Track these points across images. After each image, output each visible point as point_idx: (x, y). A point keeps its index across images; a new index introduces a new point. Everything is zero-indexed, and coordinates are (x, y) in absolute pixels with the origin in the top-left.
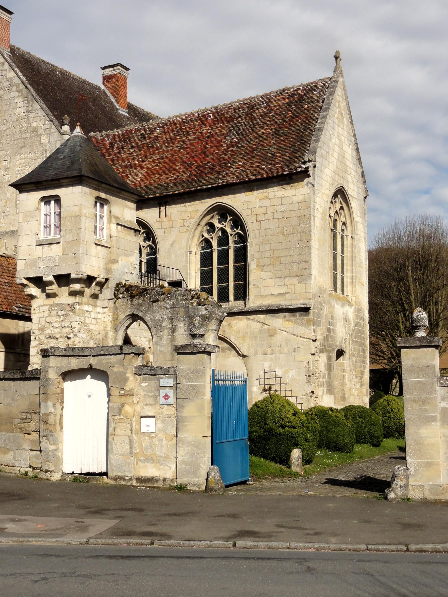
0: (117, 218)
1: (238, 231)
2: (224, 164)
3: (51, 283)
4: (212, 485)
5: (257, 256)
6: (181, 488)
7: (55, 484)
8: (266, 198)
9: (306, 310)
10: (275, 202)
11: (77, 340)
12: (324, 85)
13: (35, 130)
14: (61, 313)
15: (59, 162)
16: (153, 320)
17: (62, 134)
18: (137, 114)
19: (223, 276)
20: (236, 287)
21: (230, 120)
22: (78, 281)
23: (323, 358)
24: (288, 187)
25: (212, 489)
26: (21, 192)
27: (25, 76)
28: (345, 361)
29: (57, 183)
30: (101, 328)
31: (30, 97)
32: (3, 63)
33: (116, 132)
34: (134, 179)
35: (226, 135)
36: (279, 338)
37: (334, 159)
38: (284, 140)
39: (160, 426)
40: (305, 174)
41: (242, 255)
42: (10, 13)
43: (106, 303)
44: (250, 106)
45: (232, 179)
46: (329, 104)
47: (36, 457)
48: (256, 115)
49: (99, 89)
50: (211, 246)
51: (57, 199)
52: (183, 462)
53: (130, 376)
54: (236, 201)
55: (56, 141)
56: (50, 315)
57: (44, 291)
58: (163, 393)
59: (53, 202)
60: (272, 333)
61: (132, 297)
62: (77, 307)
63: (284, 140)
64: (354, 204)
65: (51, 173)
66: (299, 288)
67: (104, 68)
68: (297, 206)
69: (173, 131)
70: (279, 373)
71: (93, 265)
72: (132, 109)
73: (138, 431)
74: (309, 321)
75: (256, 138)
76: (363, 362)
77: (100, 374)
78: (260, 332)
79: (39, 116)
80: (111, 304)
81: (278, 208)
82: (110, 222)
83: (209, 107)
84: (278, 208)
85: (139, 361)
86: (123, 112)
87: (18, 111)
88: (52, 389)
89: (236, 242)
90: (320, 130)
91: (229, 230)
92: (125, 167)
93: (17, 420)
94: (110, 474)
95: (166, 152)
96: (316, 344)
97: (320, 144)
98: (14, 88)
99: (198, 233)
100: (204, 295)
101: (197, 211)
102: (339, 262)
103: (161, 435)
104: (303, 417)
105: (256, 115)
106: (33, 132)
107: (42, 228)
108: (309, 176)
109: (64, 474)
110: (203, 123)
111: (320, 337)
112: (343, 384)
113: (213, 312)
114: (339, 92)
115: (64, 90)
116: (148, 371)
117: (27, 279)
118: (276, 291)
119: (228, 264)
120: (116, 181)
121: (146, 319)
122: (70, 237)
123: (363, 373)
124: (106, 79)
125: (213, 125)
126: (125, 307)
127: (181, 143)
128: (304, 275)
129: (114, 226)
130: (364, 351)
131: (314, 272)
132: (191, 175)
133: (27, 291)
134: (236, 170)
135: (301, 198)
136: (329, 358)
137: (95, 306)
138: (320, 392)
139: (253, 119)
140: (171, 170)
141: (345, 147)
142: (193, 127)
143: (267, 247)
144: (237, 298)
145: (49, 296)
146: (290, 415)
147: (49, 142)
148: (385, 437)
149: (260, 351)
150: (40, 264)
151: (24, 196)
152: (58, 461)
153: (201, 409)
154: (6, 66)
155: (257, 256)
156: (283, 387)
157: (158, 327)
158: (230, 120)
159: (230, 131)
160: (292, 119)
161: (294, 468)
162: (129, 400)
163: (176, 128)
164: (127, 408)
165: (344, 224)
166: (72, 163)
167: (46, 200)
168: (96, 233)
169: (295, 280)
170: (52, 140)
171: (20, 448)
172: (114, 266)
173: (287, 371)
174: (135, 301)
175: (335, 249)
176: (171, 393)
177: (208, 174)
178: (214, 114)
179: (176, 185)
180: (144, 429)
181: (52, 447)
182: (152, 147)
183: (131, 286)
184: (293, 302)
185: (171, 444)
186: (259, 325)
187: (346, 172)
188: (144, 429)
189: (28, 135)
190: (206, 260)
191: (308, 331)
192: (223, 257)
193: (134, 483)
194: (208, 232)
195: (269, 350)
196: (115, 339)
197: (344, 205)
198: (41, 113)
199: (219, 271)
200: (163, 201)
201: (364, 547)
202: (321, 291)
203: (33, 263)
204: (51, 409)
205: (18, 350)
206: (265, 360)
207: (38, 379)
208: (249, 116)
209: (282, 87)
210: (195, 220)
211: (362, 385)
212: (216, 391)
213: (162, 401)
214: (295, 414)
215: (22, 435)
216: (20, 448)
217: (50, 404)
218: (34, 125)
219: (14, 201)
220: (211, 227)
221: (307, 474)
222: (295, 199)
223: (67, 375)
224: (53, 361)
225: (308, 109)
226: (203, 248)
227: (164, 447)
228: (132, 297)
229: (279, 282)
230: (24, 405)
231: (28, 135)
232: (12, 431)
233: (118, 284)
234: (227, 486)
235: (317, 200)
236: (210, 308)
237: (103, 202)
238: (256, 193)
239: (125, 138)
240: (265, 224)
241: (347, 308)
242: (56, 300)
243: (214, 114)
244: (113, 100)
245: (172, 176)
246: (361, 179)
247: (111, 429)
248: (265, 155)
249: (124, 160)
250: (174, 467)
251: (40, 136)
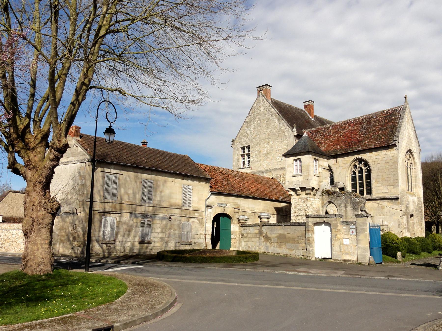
0: (321, 166)
1: (367, 168)
2: (360, 142)
3: (298, 190)
4: (370, 263)
5: (375, 177)
6: (359, 264)
7: (313, 261)
8: (378, 155)
9: (397, 199)
10: (382, 156)
11: (309, 211)
12: (400, 109)
13: (282, 131)
14: (302, 201)
15: (300, 146)
16: (338, 204)
17: (293, 132)
18: (321, 121)
19: (361, 185)
20: (367, 190)
21: (361, 124)
22: (309, 189)
23: (405, 218)
24: (388, 150)
25: (371, 264)
26: (286, 157)
27: (277, 110)
28: (414, 219)
29: (300, 154)
30: (317, 206)
31: (280, 118)
33: (313, 129)
34: (323, 148)
35: (360, 130)
36: (386, 210)
37: (406, 138)
38: (385, 132)
39: (351, 242)
40: (395, 145)
41: (369, 177)
42: (271, 86)
43: (319, 197)
44: (369, 118)
45: (364, 148)
46: (403, 117)
47: (305, 252)
48: (372, 121)
49: (303, 111)
50: (356, 174)
51: (300, 160)
52: (360, 255)
53: (339, 224)
54: (365, 156)
56: (298, 202)
57: (296, 193)
58: (351, 230)
59: (298, 161)
60: (383, 208)
61: (329, 195)
62: (309, 199)
63: (385, 132)
64: (415, 155)
65: (297, 151)
66: (394, 190)
67: (304, 102)
68: (391, 158)
69: (337, 128)
70: (387, 223)
71: (314, 183)
72: (316, 117)
73: (343, 244)
74: (399, 203)
75: (373, 131)
76: (422, 219)
77: (328, 224)
78: (378, 207)
79: (284, 126)
80: (321, 197)
81: (384, 159)
82: (319, 167)
83: (351, 118)
84: (384, 159)
85: (341, 220)
86: (313, 119)
87: (275, 123)
88: (310, 229)
89: (366, 172)
90: (400, 127)
91: (363, 167)
92: (318, 143)
93: (296, 239)
94: (333, 258)
95: (335, 137)
96: (402, 212)
97: (400, 133)
99: (350, 169)
100: (354, 193)
101: (349, 160)
102: (410, 179)
103: (351, 245)
104: (400, 240)
105: (372, 121)
107: (294, 170)
108: (396, 146)
109: (316, 258)
110: (349, 125)
111: (403, 209)
112: (413, 228)
113: (362, 201)
114: (407, 111)
115: (291, 113)
116: (346, 223)
117: (290, 189)
118: (384, 191)
119: (363, 181)
120: (320, 152)
121: (335, 203)
122: (305, 174)
123: (422, 224)
124: (305, 106)
125: (354, 126)
126: (326, 198)
127: (341, 133)
128: (396, 185)
129: (320, 169)
130: (422, 215)
131: (400, 183)
132: (346, 146)
133: (289, 193)
134: (365, 144)
135: (393, 155)
136: (407, 218)
137: (315, 198)
138: (404, 231)
139: (370, 123)
140: (338, 144)
141: (410, 133)
142: (345, 127)
143: (380, 174)
144: (367, 194)
145: (298, 195)
146: (396, 239)
148: (433, 250)
149: (378, 215)
150: (294, 183)
151: (287, 159)
152: (313, 254)
153: (366, 236)
154: (270, 107)
155: (375, 177)
156: (388, 229)
157: (340, 206)
158: (361, 124)
159: (361, 128)
160: (387, 123)
161: (398, 259)
162: (339, 233)
163: (338, 127)
164: (338, 236)
165: (411, 163)
166: (305, 146)
167: (296, 160)
168: (314, 171)
169: (392, 187)
171: (298, 249)
172: (321, 184)
173: (390, 223)
174: (330, 196)
175: (408, 174)
176: (354, 231)
177: (353, 146)
178: (353, 121)
179: (340, 150)
180: (344, 243)
181: (311, 249)
182: (329, 135)
183: (328, 191)
184: (392, 196)
185: (355, 248)
186: (377, 205)
187: (411, 143)
188: (344, 243)
189: (280, 132)
190: (354, 179)
191: (399, 207)
192: (361, 178)
193: (342, 261)
194: (354, 168)
195: (382, 214)
196: (323, 210)
197: (411, 156)
198: (285, 124)
199: (359, 183)
200: (335, 157)
201: (433, 281)
202: (403, 191)
203: (291, 183)
204: (310, 236)
205: (281, 214)
206: (380, 218)
207: (305, 225)
208: (369, 122)
209: (382, 110)
210: (349, 164)
211: (421, 229)
212: (371, 230)
213: (351, 233)
214: (398, 239)
215: (298, 244)
216: (298, 249)
217: (310, 234)
218: (282, 128)
220: (356, 167)
221: (404, 262)
222: (391, 155)
223: (316, 224)
224: (310, 219)
225: (394, 119)
226: (352, 175)
227: (353, 249)
228: (329, 195)
229: (385, 188)
230: (299, 234)
231: (280, 132)
232: (295, 243)
233: (323, 190)
234: (376, 264)
235: (400, 155)
236: (360, 199)
237: (316, 160)
238: (374, 153)
239: (317, 132)
240: (378, 165)
241: (414, 197)
242: (300, 196)
243: (353, 121)
244: (308, 115)
245: (338, 147)
246: (418, 144)
247: (332, 243)
248: (377, 138)
249: (317, 140)
250: (356, 256)
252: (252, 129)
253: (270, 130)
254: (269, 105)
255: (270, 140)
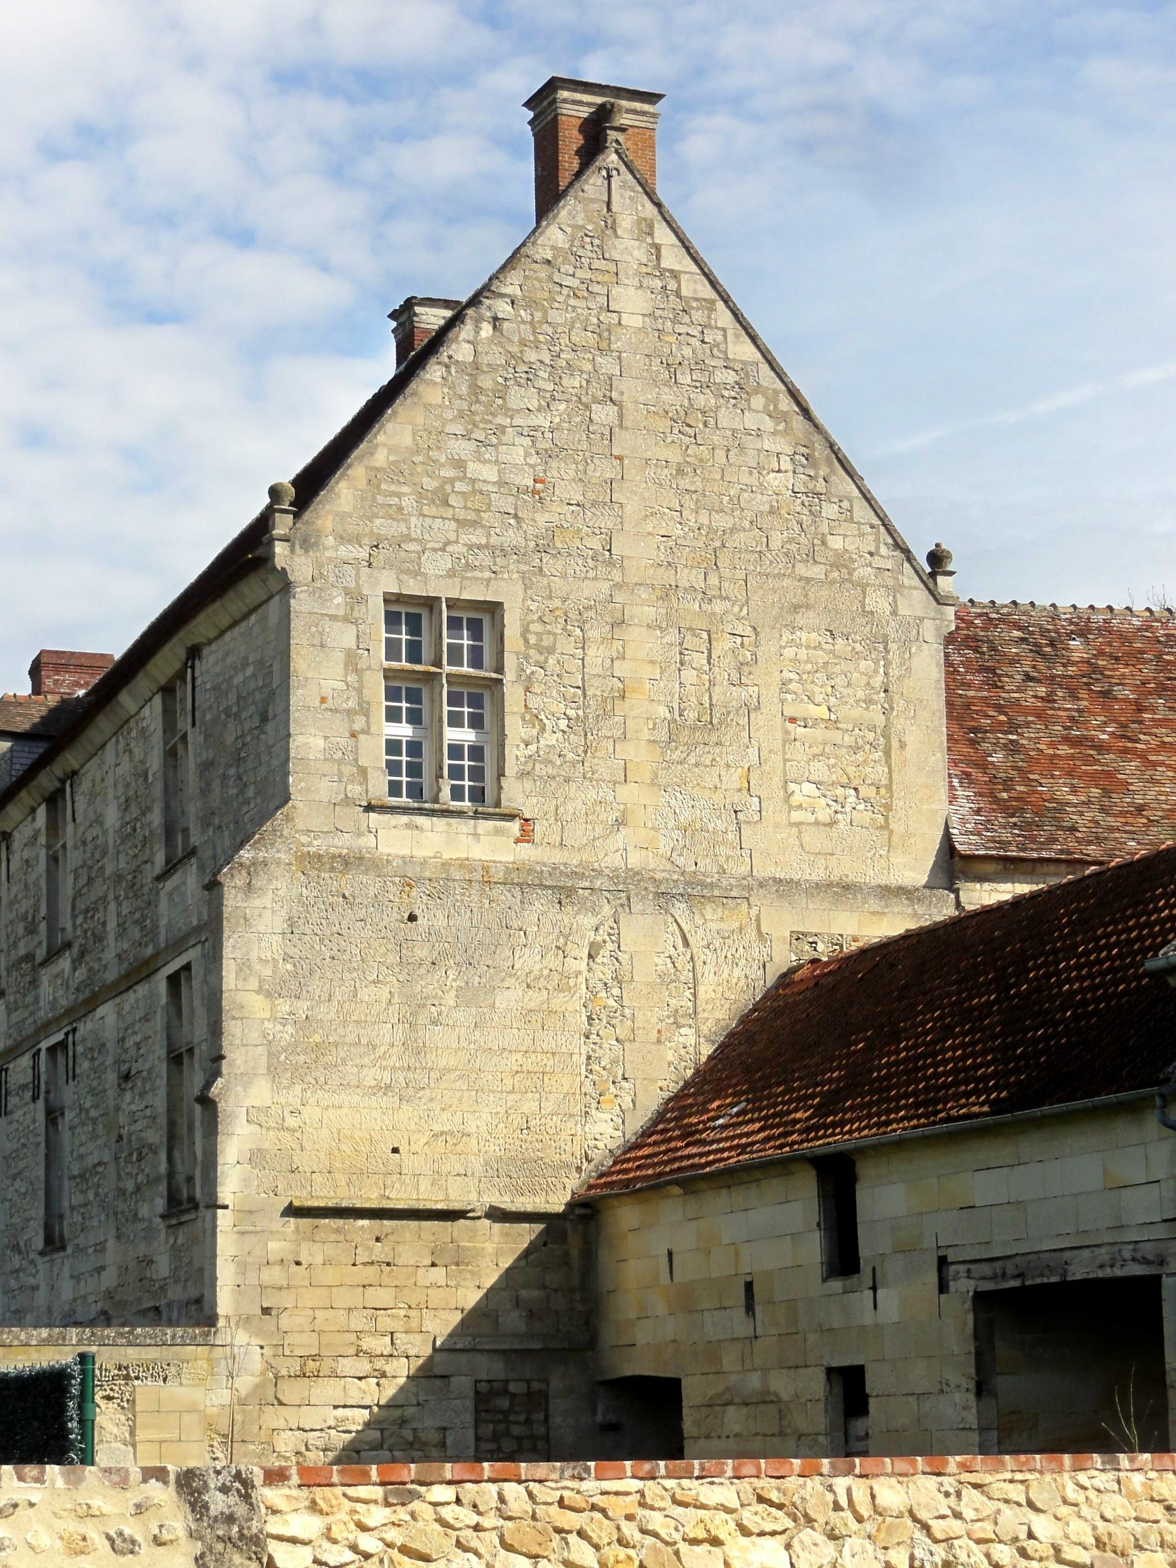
13: (841, 562)
32: (713, 302)
55: (922, 619)
98: (758, 402)
106: (835, 565)
147: (894, 613)
170: (902, 611)
218: (836, 543)
219: (777, 781)
231: (817, 572)
251: (863, 586)
252: (516, 452)
253: (721, 521)
254: (708, 292)
255: (718, 607)
